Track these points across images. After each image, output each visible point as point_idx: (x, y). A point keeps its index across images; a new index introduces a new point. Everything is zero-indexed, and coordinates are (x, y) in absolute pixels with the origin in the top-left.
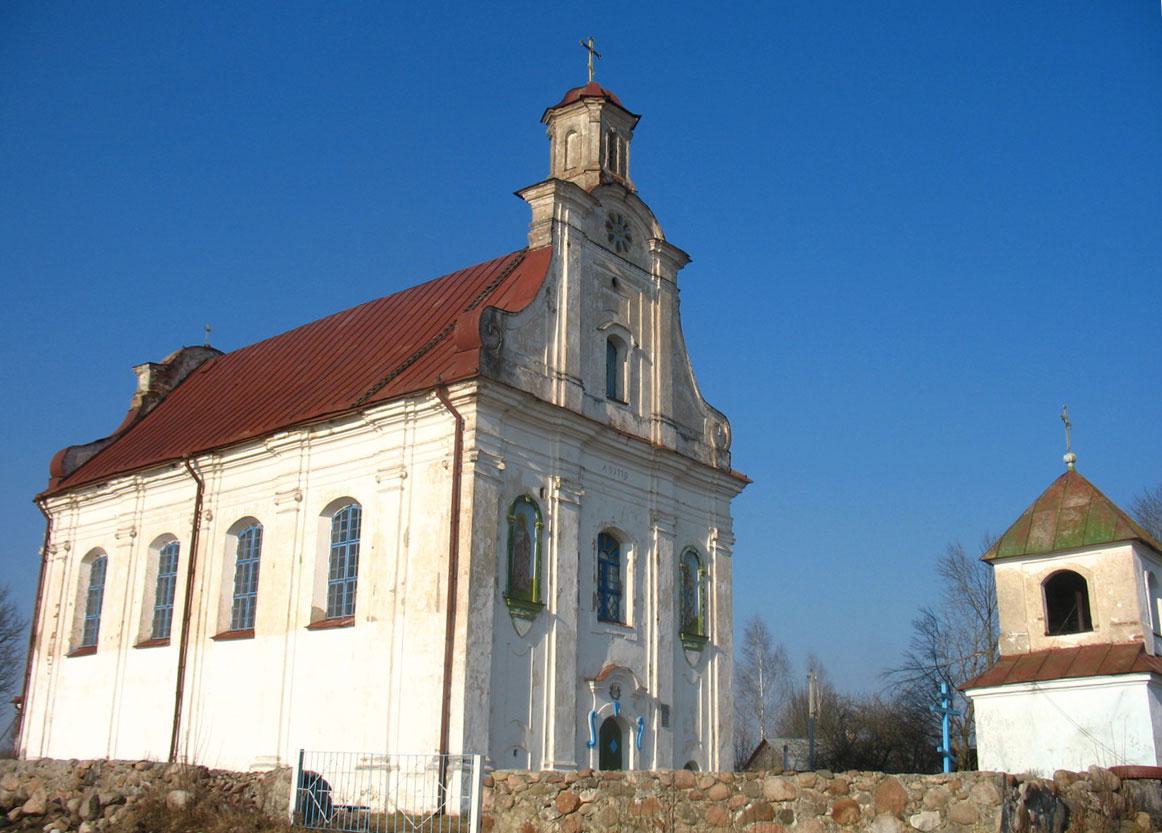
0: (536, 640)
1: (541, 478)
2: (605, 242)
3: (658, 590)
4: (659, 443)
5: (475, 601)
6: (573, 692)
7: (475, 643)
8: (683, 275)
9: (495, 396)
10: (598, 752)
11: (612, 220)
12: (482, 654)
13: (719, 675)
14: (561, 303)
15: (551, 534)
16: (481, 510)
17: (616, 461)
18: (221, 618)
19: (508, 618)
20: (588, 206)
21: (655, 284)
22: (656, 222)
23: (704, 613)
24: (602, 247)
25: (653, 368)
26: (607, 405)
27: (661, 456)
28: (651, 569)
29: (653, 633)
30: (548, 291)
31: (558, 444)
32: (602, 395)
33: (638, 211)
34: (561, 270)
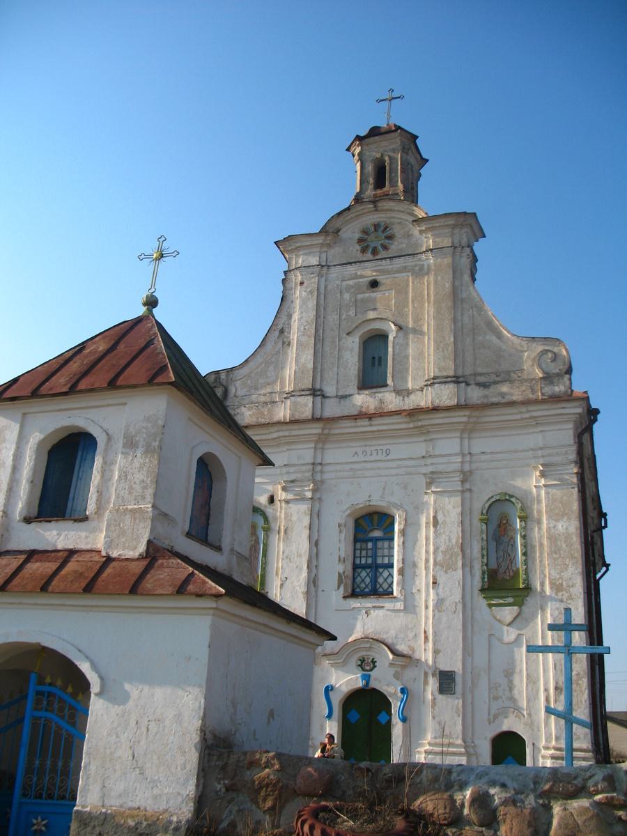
1: (270, 488)
2: (360, 256)
3: (435, 552)
17: (368, 443)
20: (321, 241)
24: (351, 263)
26: (357, 396)
27: (420, 420)
32: (352, 387)
33: (396, 208)
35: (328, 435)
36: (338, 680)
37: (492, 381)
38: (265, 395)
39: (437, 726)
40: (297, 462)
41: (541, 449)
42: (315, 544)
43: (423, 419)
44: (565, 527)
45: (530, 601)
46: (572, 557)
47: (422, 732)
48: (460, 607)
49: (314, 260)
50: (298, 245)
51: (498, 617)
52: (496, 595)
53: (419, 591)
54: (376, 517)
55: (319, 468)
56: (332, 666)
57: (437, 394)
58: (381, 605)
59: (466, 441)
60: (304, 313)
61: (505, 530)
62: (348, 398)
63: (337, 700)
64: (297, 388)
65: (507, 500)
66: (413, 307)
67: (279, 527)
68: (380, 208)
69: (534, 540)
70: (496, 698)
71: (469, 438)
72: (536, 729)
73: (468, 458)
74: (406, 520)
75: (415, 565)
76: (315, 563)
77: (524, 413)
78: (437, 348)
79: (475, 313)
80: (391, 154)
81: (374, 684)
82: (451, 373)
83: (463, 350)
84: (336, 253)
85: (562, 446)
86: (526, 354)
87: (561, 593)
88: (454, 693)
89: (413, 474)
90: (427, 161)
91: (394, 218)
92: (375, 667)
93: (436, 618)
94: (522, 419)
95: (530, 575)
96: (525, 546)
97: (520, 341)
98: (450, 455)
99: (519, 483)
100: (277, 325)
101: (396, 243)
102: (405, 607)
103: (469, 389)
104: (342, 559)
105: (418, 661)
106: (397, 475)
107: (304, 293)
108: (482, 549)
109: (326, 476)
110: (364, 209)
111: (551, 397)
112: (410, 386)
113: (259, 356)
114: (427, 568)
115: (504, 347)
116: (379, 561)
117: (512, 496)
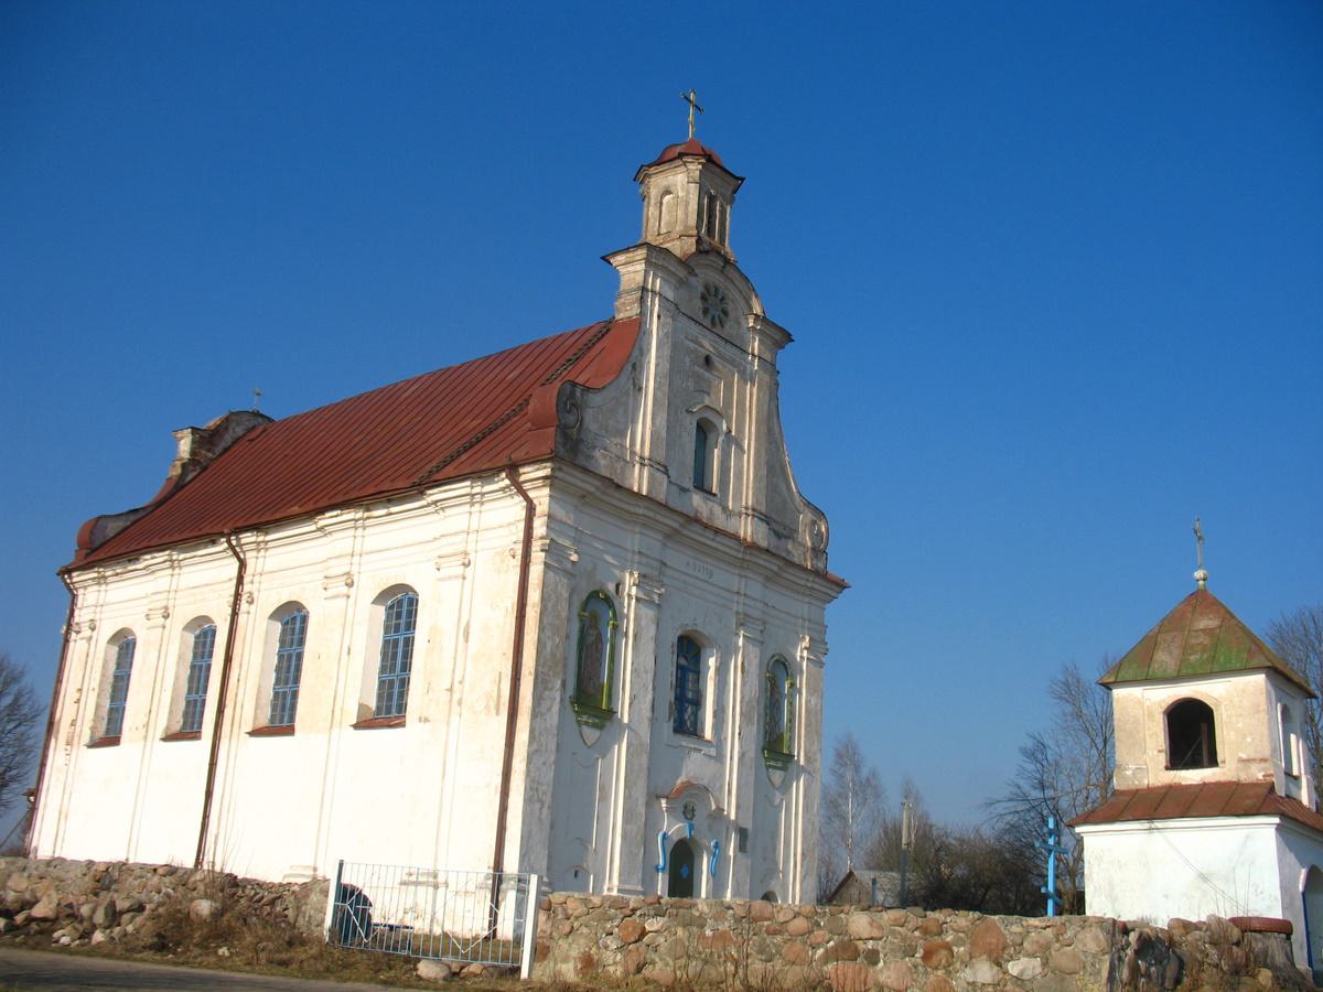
0: (605, 750)
1: (617, 572)
2: (699, 316)
3: (741, 702)
4: (749, 539)
5: (539, 704)
6: (642, 810)
7: (537, 751)
8: (784, 357)
9: (569, 479)
10: (667, 877)
11: (708, 292)
12: (544, 763)
13: (805, 797)
14: (647, 380)
15: (626, 635)
16: (550, 605)
18: (259, 711)
19: (576, 725)
20: (682, 276)
21: (752, 363)
22: (756, 296)
23: (791, 729)
25: (746, 456)
26: (694, 496)
27: (750, 554)
28: (735, 678)
29: (733, 748)
30: (634, 366)
31: (638, 536)
32: (689, 484)
34: (650, 344)
68: (726, 272)
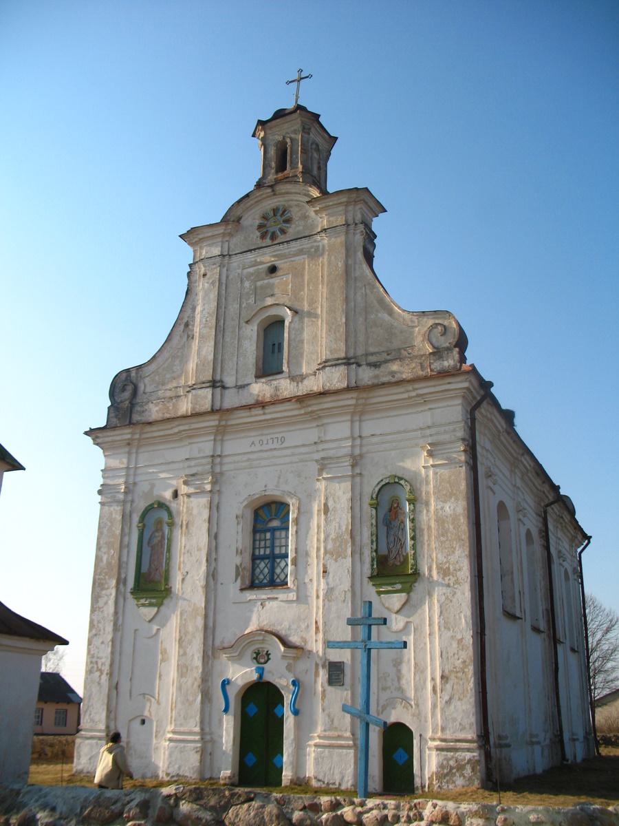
2: (260, 243)
5: (97, 602)
6: (198, 662)
7: (96, 635)
12: (102, 643)
16: (105, 531)
17: (266, 432)
20: (222, 231)
24: (250, 251)
26: (254, 385)
27: (309, 406)
32: (250, 377)
33: (293, 191)
35: (225, 426)
36: (234, 673)
37: (383, 359)
38: (170, 390)
39: (327, 718)
40: (198, 456)
41: (429, 427)
42: (214, 536)
43: (313, 405)
44: (452, 508)
45: (419, 587)
46: (460, 539)
47: (312, 726)
48: (349, 595)
49: (216, 251)
50: (201, 237)
51: (387, 605)
52: (384, 582)
53: (311, 580)
54: (273, 506)
55: (218, 460)
56: (229, 660)
57: (328, 377)
58: (276, 596)
59: (357, 424)
60: (206, 305)
61: (396, 513)
62: (246, 388)
63: (233, 692)
64: (199, 381)
65: (395, 482)
66: (309, 290)
67: (182, 521)
68: (277, 193)
69: (422, 523)
70: (384, 689)
71: (360, 421)
72: (423, 719)
73: (358, 442)
74: (299, 509)
75: (307, 554)
76: (214, 556)
77: (410, 391)
78: (329, 330)
79: (368, 291)
80: (293, 136)
81: (268, 677)
82: (343, 355)
83: (355, 331)
84: (237, 242)
85: (450, 423)
86: (417, 329)
87: (448, 578)
88: (343, 685)
89: (307, 461)
90: (336, 139)
91: (292, 200)
92: (269, 659)
93: (325, 608)
94: (410, 398)
95: (419, 560)
96: (414, 530)
97: (410, 317)
98: (341, 440)
99: (408, 464)
100: (182, 319)
101: (293, 226)
102: (298, 597)
103: (360, 369)
104: (239, 551)
105: (310, 652)
106: (291, 463)
107: (206, 284)
108: (372, 535)
109: (225, 468)
110: (262, 195)
111: (439, 373)
112: (304, 370)
113: (166, 351)
114: (318, 557)
115: (395, 324)
116: (277, 551)
117: (402, 479)
